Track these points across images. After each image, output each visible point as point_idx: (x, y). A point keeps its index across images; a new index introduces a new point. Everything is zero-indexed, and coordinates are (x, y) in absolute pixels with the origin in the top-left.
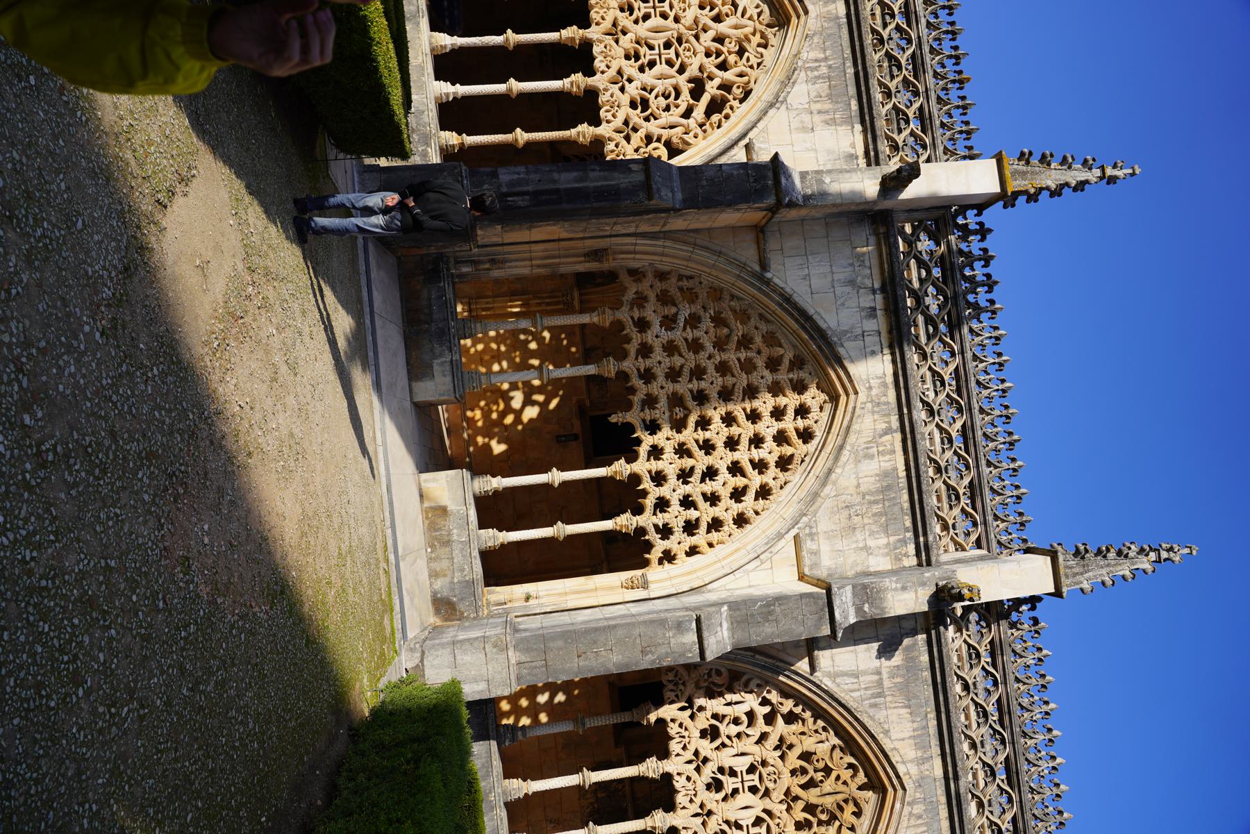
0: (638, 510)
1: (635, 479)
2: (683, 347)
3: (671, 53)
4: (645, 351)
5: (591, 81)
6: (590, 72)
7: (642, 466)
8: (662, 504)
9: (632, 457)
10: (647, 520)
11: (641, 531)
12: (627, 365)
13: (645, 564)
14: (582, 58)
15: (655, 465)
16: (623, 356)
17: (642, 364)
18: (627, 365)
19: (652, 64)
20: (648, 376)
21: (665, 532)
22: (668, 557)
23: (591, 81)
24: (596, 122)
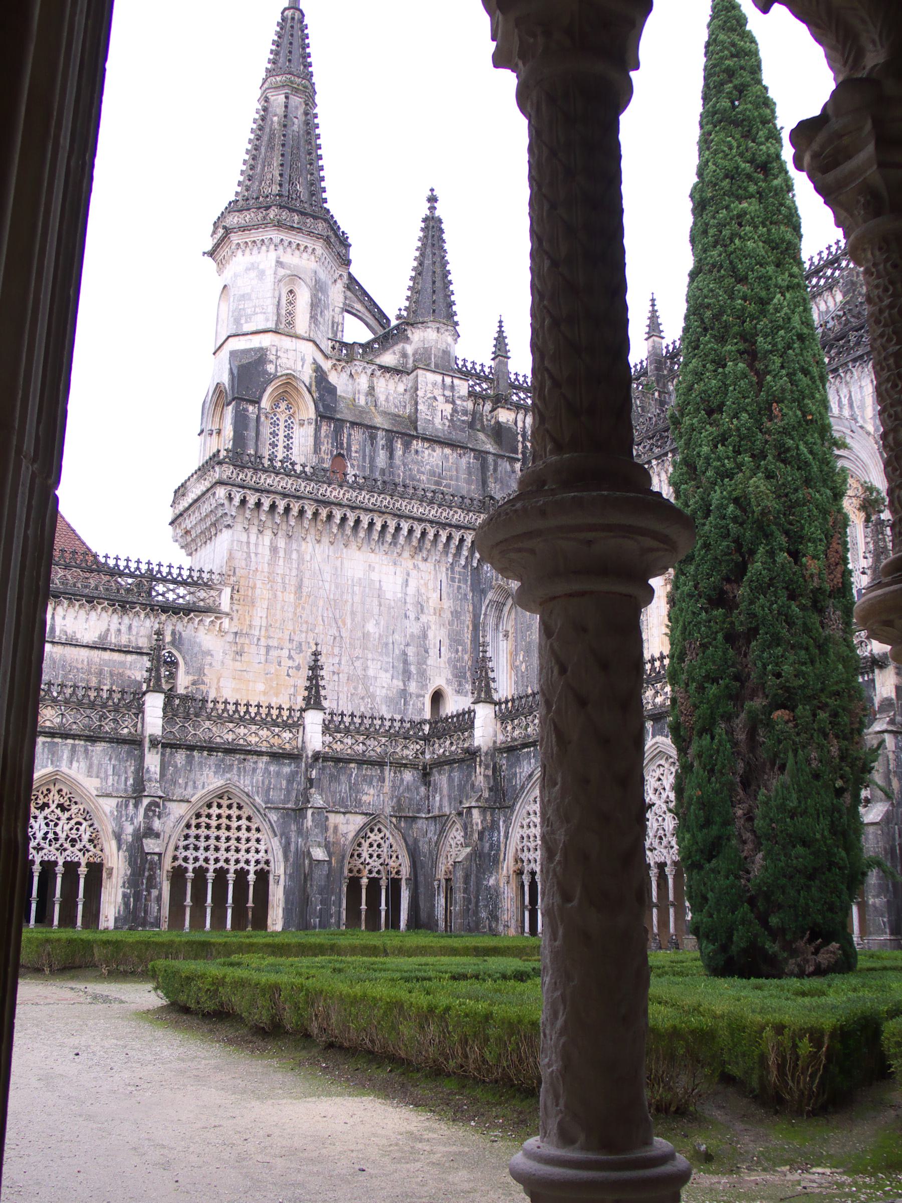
0: (248, 872)
1: (236, 871)
2: (186, 842)
3: (52, 824)
4: (186, 859)
5: (61, 863)
6: (55, 863)
7: (232, 868)
8: (247, 862)
9: (227, 871)
10: (252, 868)
11: (256, 872)
12: (191, 867)
13: (268, 872)
14: (71, 867)
15: (232, 862)
16: (186, 869)
17: (191, 861)
18: (191, 867)
19: (55, 833)
20: (196, 859)
21: (257, 862)
22: (267, 862)
23: (61, 863)
24: (78, 864)
